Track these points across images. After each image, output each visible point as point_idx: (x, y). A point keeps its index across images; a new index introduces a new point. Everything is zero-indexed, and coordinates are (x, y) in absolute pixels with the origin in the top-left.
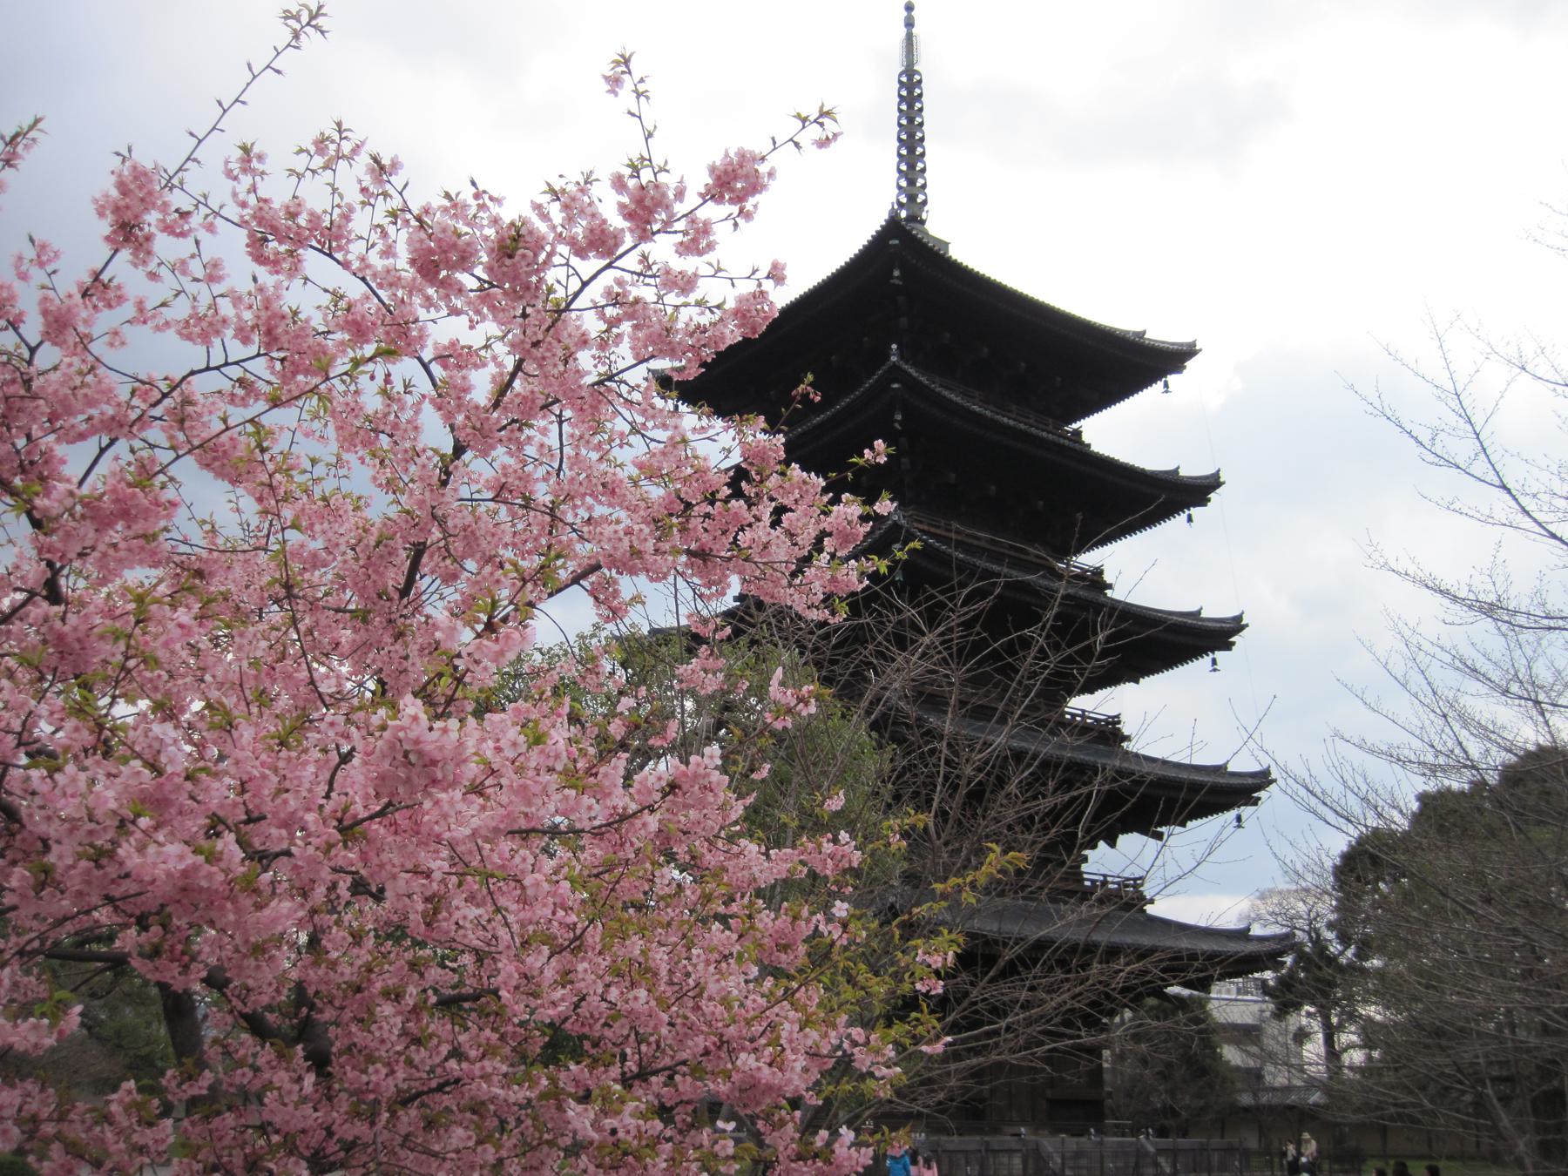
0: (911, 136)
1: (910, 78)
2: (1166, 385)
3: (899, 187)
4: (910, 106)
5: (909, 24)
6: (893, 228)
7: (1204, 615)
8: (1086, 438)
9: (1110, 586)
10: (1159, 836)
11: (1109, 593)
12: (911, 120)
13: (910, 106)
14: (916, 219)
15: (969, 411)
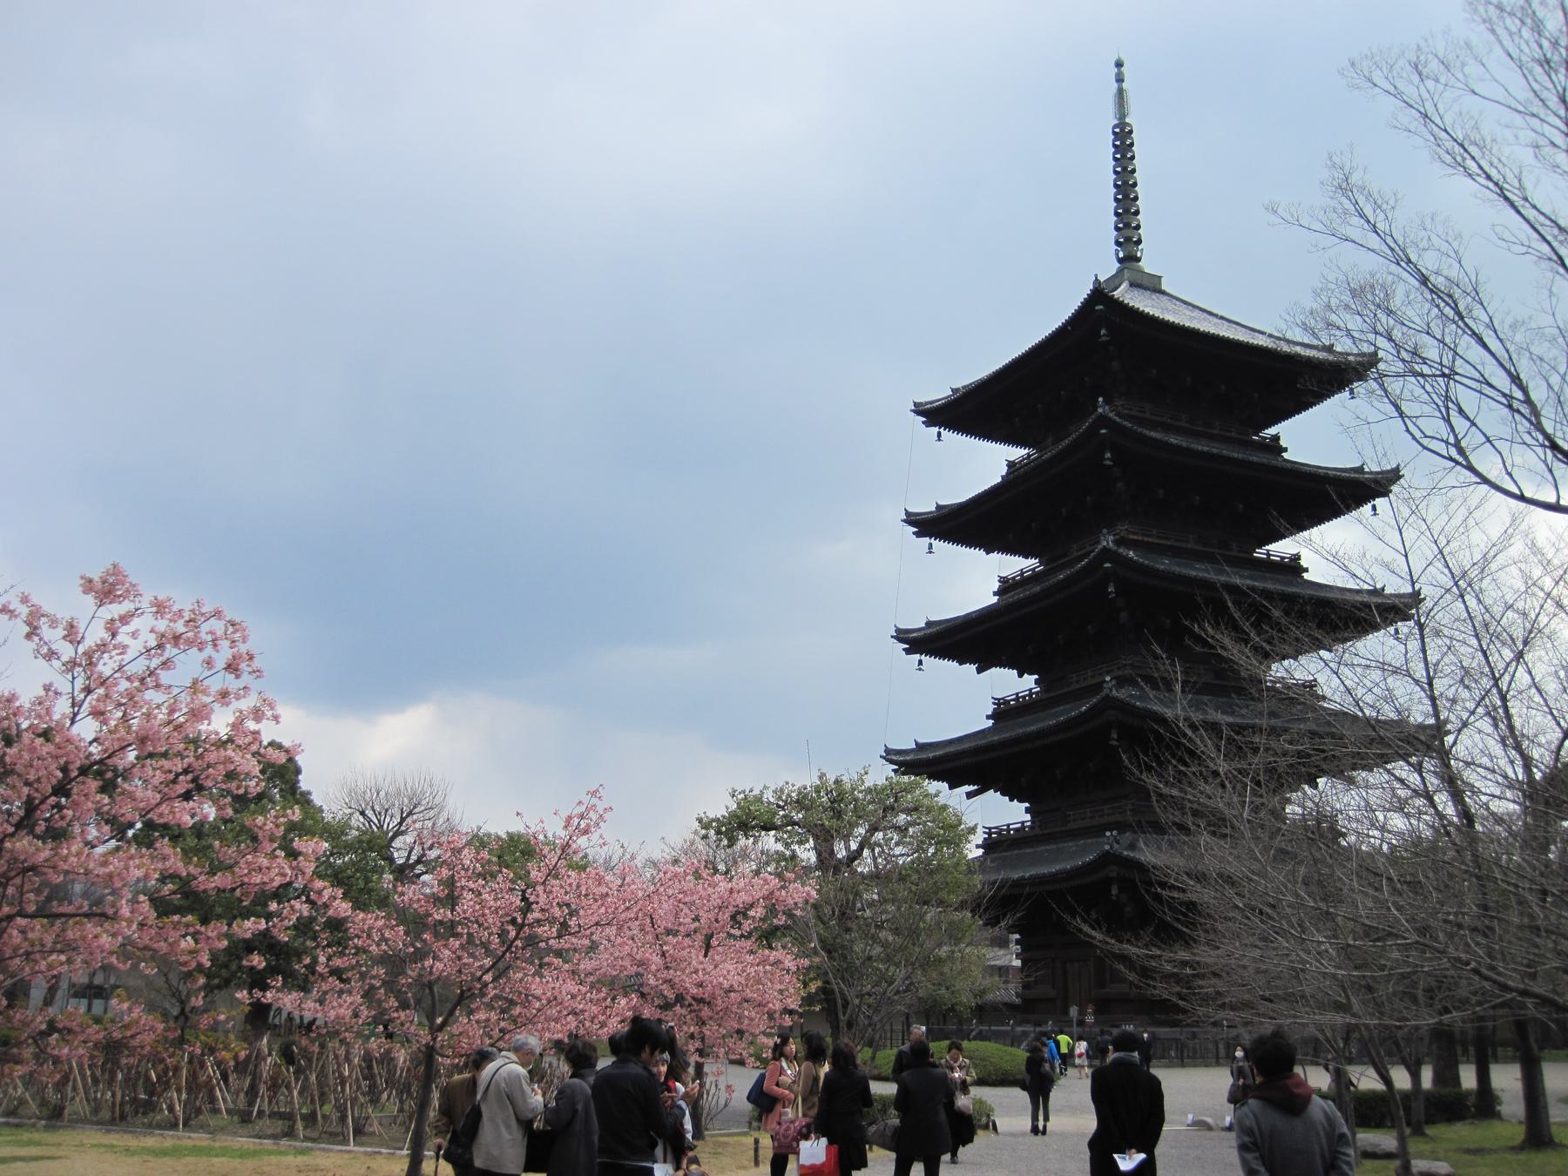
0: (1125, 183)
1: (1122, 130)
2: (1352, 392)
3: (1117, 229)
4: (1124, 156)
5: (1120, 79)
6: (1100, 294)
7: (1388, 591)
8: (1283, 443)
9: (1306, 570)
10: (1351, 781)
11: (1306, 576)
12: (1125, 169)
13: (1124, 156)
14: (1129, 260)
15: (1167, 444)
